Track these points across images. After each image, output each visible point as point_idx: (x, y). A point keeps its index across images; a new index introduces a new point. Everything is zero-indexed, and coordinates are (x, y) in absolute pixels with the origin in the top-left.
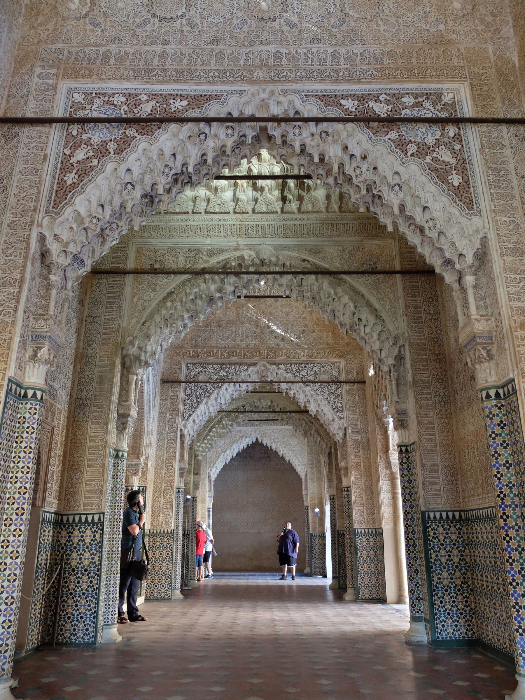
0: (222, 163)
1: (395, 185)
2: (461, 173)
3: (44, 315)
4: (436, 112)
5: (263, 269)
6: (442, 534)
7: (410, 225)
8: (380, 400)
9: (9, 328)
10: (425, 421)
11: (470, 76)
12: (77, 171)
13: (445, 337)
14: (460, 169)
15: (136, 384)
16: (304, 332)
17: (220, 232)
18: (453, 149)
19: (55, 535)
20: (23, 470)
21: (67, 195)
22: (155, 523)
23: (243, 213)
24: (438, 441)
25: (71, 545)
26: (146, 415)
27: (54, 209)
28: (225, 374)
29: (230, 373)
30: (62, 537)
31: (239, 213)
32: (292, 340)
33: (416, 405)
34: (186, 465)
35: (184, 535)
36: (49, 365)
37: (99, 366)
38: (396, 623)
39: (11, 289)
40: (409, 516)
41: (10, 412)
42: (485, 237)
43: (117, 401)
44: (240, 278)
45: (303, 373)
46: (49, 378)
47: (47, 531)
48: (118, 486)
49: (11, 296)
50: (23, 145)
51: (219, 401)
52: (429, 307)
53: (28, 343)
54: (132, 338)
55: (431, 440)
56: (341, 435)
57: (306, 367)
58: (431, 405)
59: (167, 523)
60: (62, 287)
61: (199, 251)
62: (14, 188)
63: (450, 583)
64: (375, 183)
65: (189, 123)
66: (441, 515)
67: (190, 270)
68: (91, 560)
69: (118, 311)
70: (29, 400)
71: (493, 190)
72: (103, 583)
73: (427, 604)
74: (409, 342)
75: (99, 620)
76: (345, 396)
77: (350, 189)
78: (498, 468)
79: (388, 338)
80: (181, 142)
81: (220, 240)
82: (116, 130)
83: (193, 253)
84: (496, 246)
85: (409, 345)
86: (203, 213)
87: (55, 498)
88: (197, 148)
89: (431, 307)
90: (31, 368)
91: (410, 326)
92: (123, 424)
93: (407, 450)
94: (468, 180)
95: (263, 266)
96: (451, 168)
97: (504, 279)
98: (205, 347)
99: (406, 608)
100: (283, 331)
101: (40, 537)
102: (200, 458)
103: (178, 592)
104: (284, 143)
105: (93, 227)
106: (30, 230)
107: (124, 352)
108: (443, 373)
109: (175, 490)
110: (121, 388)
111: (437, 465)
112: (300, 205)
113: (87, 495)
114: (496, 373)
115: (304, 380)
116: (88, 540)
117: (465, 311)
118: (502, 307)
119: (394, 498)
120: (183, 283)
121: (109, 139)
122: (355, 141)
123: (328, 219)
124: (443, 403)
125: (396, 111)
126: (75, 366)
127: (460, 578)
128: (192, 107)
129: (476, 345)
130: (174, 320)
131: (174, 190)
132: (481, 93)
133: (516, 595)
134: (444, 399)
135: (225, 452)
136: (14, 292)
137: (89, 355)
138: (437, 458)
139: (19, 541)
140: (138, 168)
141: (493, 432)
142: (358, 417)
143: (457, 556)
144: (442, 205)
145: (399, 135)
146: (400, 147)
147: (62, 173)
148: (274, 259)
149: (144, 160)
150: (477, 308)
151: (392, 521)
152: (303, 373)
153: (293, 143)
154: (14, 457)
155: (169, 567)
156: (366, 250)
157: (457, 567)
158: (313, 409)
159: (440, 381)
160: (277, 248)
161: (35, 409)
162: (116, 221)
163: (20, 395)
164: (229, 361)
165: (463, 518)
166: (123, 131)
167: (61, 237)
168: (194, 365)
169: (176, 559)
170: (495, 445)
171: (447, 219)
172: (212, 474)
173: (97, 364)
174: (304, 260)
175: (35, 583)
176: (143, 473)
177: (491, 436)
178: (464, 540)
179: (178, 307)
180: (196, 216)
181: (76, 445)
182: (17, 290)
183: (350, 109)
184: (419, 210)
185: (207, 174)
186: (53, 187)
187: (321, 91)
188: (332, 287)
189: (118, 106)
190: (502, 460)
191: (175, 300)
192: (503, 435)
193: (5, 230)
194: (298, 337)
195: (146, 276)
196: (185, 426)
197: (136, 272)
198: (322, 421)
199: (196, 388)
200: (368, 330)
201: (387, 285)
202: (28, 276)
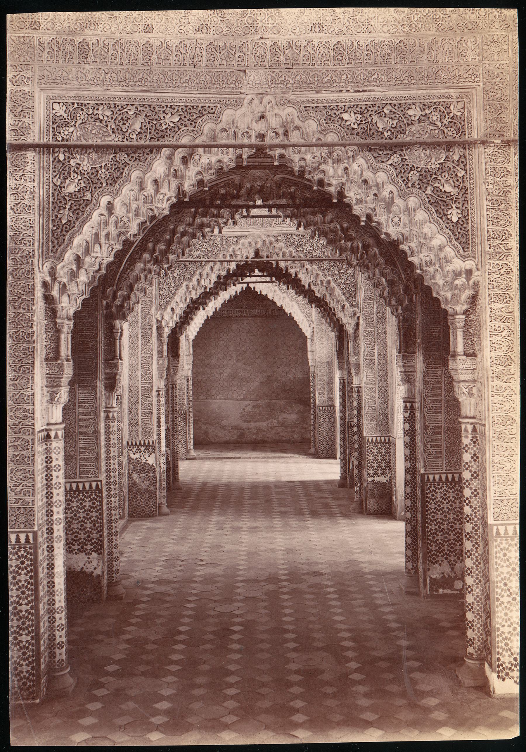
18: (456, 175)
21: (64, 235)
51: (203, 282)
55: (437, 401)
94: (468, 215)
109: (155, 394)
111: (440, 427)
125: (400, 127)
132: (493, 102)
147: (55, 208)
166: (112, 156)
183: (352, 125)
189: (104, 122)
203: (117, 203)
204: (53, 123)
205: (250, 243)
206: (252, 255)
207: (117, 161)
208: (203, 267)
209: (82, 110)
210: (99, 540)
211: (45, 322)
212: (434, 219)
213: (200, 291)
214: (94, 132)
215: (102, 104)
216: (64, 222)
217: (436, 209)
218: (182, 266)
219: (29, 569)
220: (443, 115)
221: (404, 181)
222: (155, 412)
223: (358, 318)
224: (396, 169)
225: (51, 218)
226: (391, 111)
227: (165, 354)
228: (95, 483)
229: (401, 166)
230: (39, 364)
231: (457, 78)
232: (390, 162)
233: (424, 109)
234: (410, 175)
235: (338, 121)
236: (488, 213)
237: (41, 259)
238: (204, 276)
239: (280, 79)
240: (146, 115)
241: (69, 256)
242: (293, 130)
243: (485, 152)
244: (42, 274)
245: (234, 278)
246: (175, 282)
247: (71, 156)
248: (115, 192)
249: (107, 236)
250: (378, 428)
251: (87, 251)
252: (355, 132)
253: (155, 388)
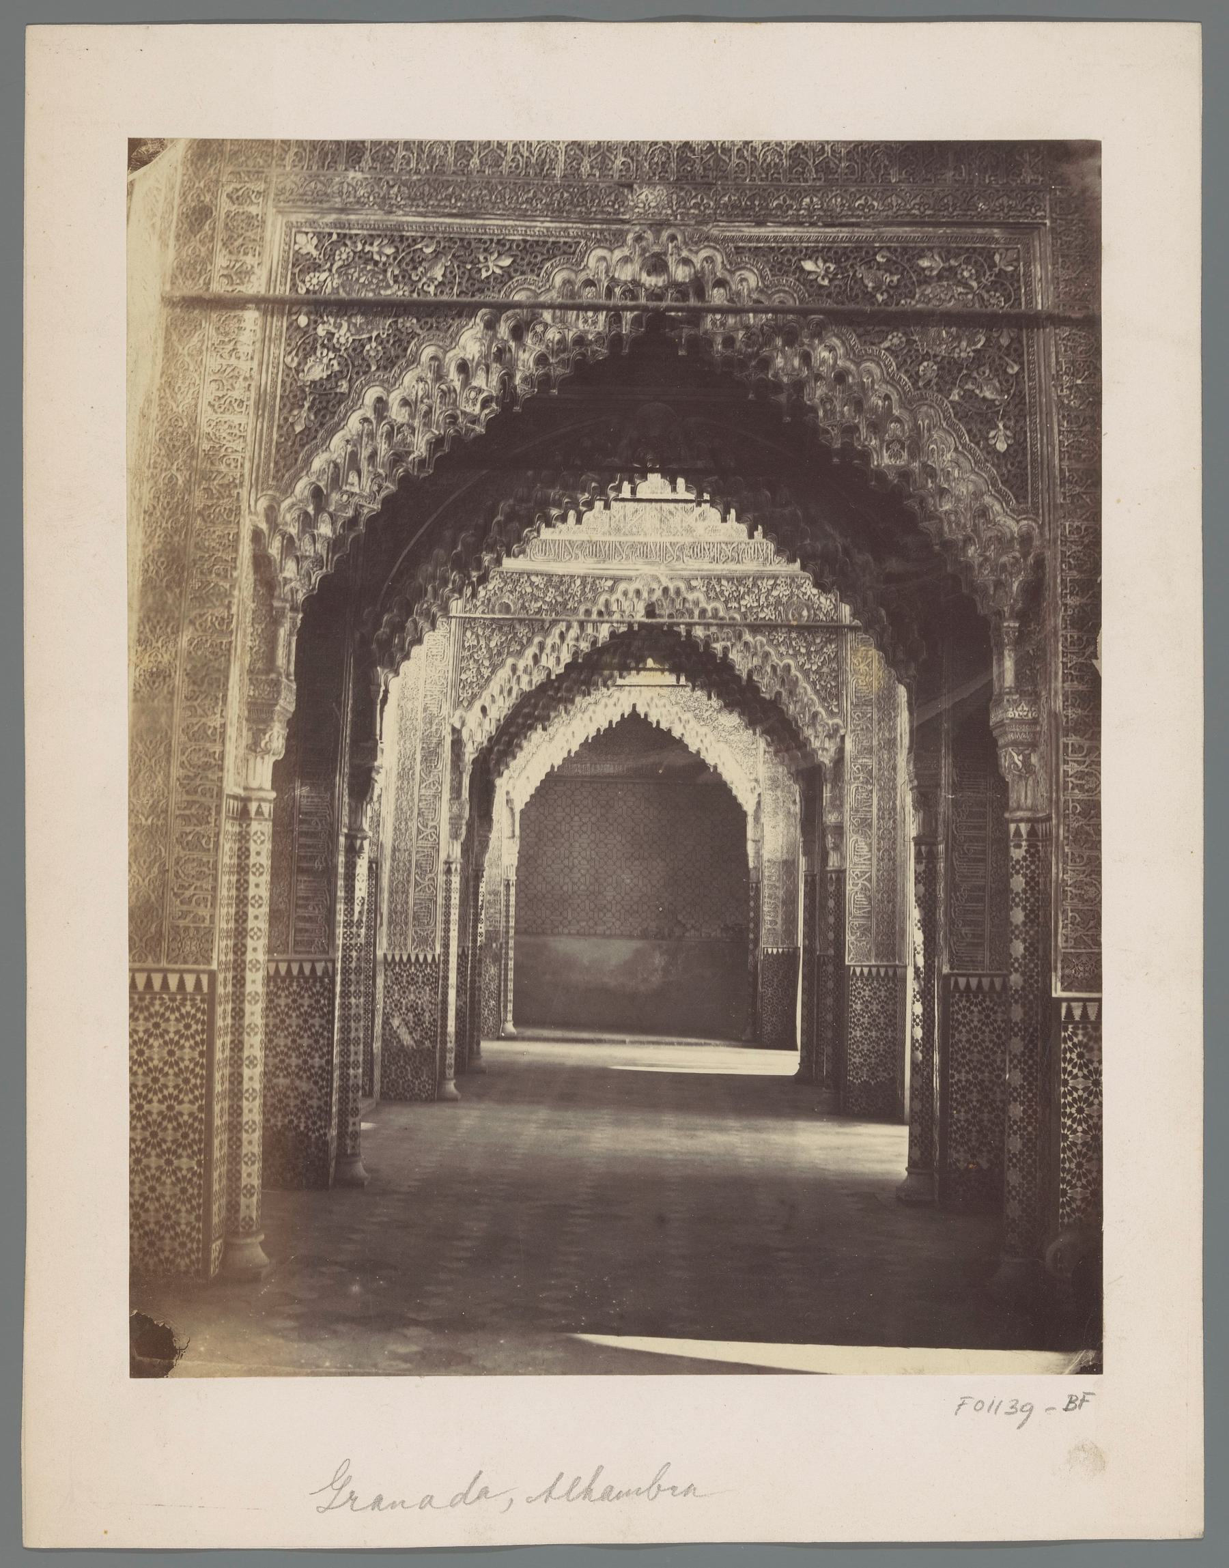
21: (297, 453)
51: (543, 661)
57: (754, 584)
66: (980, 982)
109: (441, 867)
125: (905, 285)
189: (381, 265)
203: (394, 399)
204: (293, 265)
205: (638, 592)
206: (640, 616)
207: (398, 329)
208: (546, 632)
209: (346, 245)
210: (324, 1070)
211: (253, 606)
212: (964, 446)
213: (538, 678)
214: (362, 280)
215: (379, 236)
216: (298, 429)
218: (506, 629)
219: (198, 1038)
222: (440, 901)
223: (843, 738)
224: (897, 357)
225: (276, 424)
226: (888, 260)
227: (465, 794)
230: (237, 677)
232: (886, 344)
233: (948, 260)
234: (921, 368)
235: (794, 273)
237: (253, 490)
238: (548, 650)
240: (454, 255)
241: (302, 487)
242: (714, 286)
243: (1056, 334)
244: (254, 518)
245: (606, 673)
246: (490, 658)
248: (392, 381)
249: (373, 456)
250: (873, 949)
251: (336, 481)
253: (443, 856)
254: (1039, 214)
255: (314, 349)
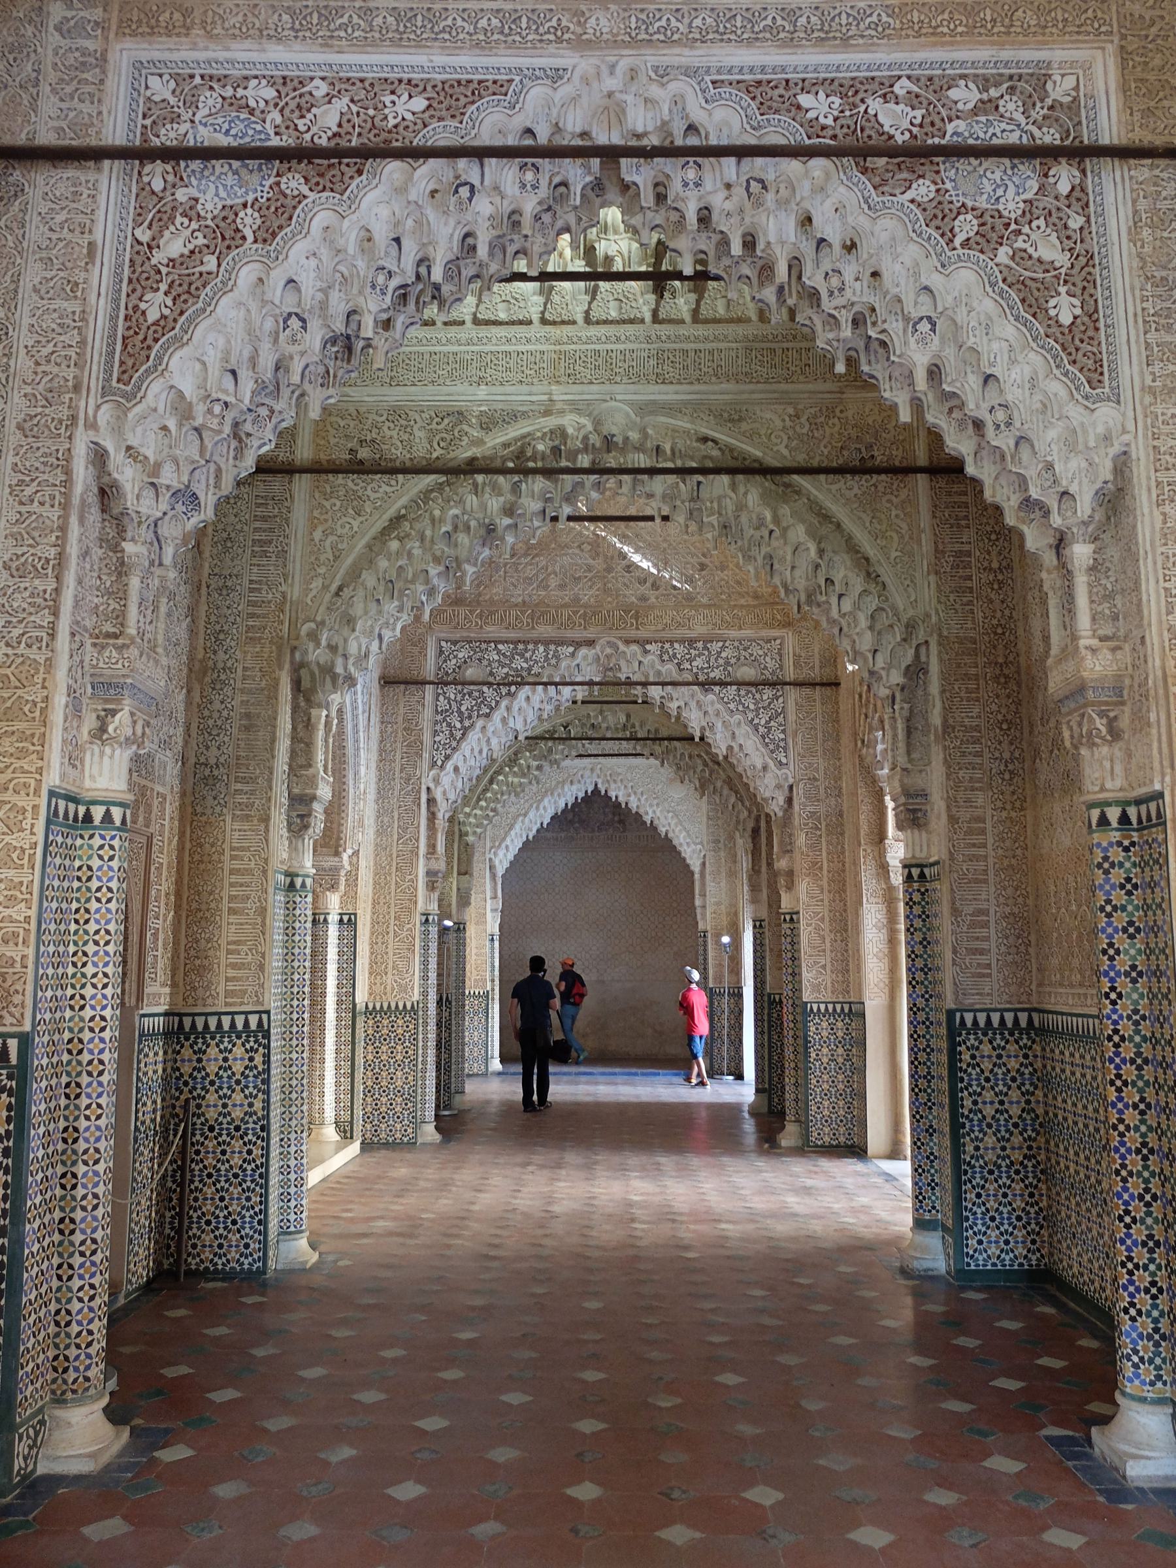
0: (511, 250)
1: (921, 319)
2: (1079, 292)
3: (116, 636)
4: (1030, 127)
5: (611, 461)
6: (990, 1057)
7: (951, 410)
8: (871, 729)
9: (41, 676)
10: (964, 814)
11: (1120, 26)
12: (170, 286)
13: (1020, 624)
14: (1078, 280)
15: (328, 724)
16: (703, 567)
17: (509, 369)
18: (1066, 227)
19: (170, 1056)
20: (94, 981)
21: (149, 348)
22: (378, 989)
23: (563, 322)
24: (991, 860)
25: (203, 1078)
26: (351, 760)
27: (121, 386)
28: (525, 665)
29: (536, 662)
30: (183, 1061)
31: (554, 323)
32: (675, 587)
33: (948, 778)
34: (441, 865)
35: (439, 1002)
36: (134, 747)
37: (242, 691)
38: (884, 1215)
39: (37, 582)
40: (921, 1016)
41: (58, 861)
42: (1125, 453)
43: (286, 768)
44: (556, 481)
45: (698, 662)
46: (140, 766)
47: (151, 1054)
48: (296, 951)
49: (39, 601)
50: (36, 219)
51: (511, 724)
52: (989, 553)
53: (85, 701)
54: (313, 625)
55: (977, 858)
56: (781, 800)
58: (980, 780)
59: (404, 989)
60: (152, 563)
61: (460, 416)
62: (24, 331)
63: (998, 1157)
64: (873, 310)
65: (431, 160)
67: (440, 464)
68: (246, 1108)
69: (280, 563)
70: (95, 828)
71: (1152, 337)
72: (275, 1152)
73: (949, 1199)
74: (940, 635)
75: (270, 1225)
76: (791, 717)
77: (814, 317)
78: (1112, 980)
79: (891, 626)
80: (413, 207)
81: (508, 389)
82: (255, 179)
83: (446, 421)
84: (1149, 478)
85: (940, 644)
86: (469, 324)
87: (163, 985)
88: (452, 222)
89: (994, 553)
90: (96, 758)
91: (943, 599)
92: (301, 817)
93: (922, 876)
94: (1096, 311)
95: (609, 451)
96: (1057, 277)
97: (1160, 559)
98: (479, 603)
99: (903, 1169)
100: (655, 565)
101: (139, 1069)
102: (471, 839)
103: (430, 1128)
104: (661, 198)
105: (214, 423)
106: (70, 438)
107: (297, 655)
108: (1013, 707)
109: (418, 919)
110: (295, 738)
111: (985, 912)
112: (698, 302)
113: (231, 973)
114: (1127, 770)
115: (701, 678)
116: (238, 1067)
117: (1067, 619)
118: (1150, 625)
119: (892, 941)
120: (426, 495)
121: (241, 201)
122: (829, 205)
123: (764, 339)
124: (1007, 776)
125: (932, 124)
126: (189, 692)
127: (1020, 1148)
128: (437, 114)
129: (1085, 706)
130: (406, 581)
131: (400, 321)
133: (1129, 1242)
134: (1011, 767)
135: (525, 815)
136: (45, 591)
137: (220, 665)
138: (989, 897)
139: (98, 1128)
140: (312, 275)
141: (1108, 902)
142: (821, 763)
143: (1018, 1102)
144: (1027, 370)
145: (938, 191)
146: (938, 222)
147: (134, 291)
148: (634, 436)
149: (324, 253)
150: (1094, 619)
151: (887, 990)
152: (698, 662)
153: (680, 205)
154: (75, 954)
155: (411, 1078)
156: (850, 414)
157: (1016, 1125)
158: (720, 743)
159: (1005, 726)
160: (645, 409)
161: (112, 847)
162: (267, 401)
163: (76, 819)
164: (534, 634)
165: (1036, 1024)
166: (272, 180)
167: (142, 450)
168: (455, 643)
169: (424, 1062)
170: (1110, 930)
171: (1039, 405)
172: (497, 863)
173: (239, 685)
174: (705, 439)
175: (135, 1161)
176: (347, 885)
177: (1102, 909)
178: (1035, 1070)
179: (416, 552)
180: (453, 331)
181: (202, 866)
182: (51, 585)
183: (822, 120)
184: (974, 381)
185: (478, 276)
186: (114, 328)
187: (752, 70)
188: (768, 505)
189: (257, 113)
190: (1123, 963)
191: (408, 535)
192: (1130, 908)
193: (13, 438)
194: (690, 580)
195: (340, 479)
196: (437, 781)
197: (317, 469)
198: (740, 770)
199: (459, 697)
200: (847, 605)
201: (895, 500)
202: (73, 550)
204: (144, 116)
209: (211, 88)
215: (256, 77)
217: (1022, 295)
220: (1029, 102)
221: (942, 235)
224: (925, 210)
228: (257, 1016)
229: (934, 204)
231: (1060, 26)
234: (957, 223)
236: (1145, 305)
239: (657, 25)
240: (352, 101)
247: (179, 183)
252: (830, 132)
254: (1103, 29)
255: (172, 219)
